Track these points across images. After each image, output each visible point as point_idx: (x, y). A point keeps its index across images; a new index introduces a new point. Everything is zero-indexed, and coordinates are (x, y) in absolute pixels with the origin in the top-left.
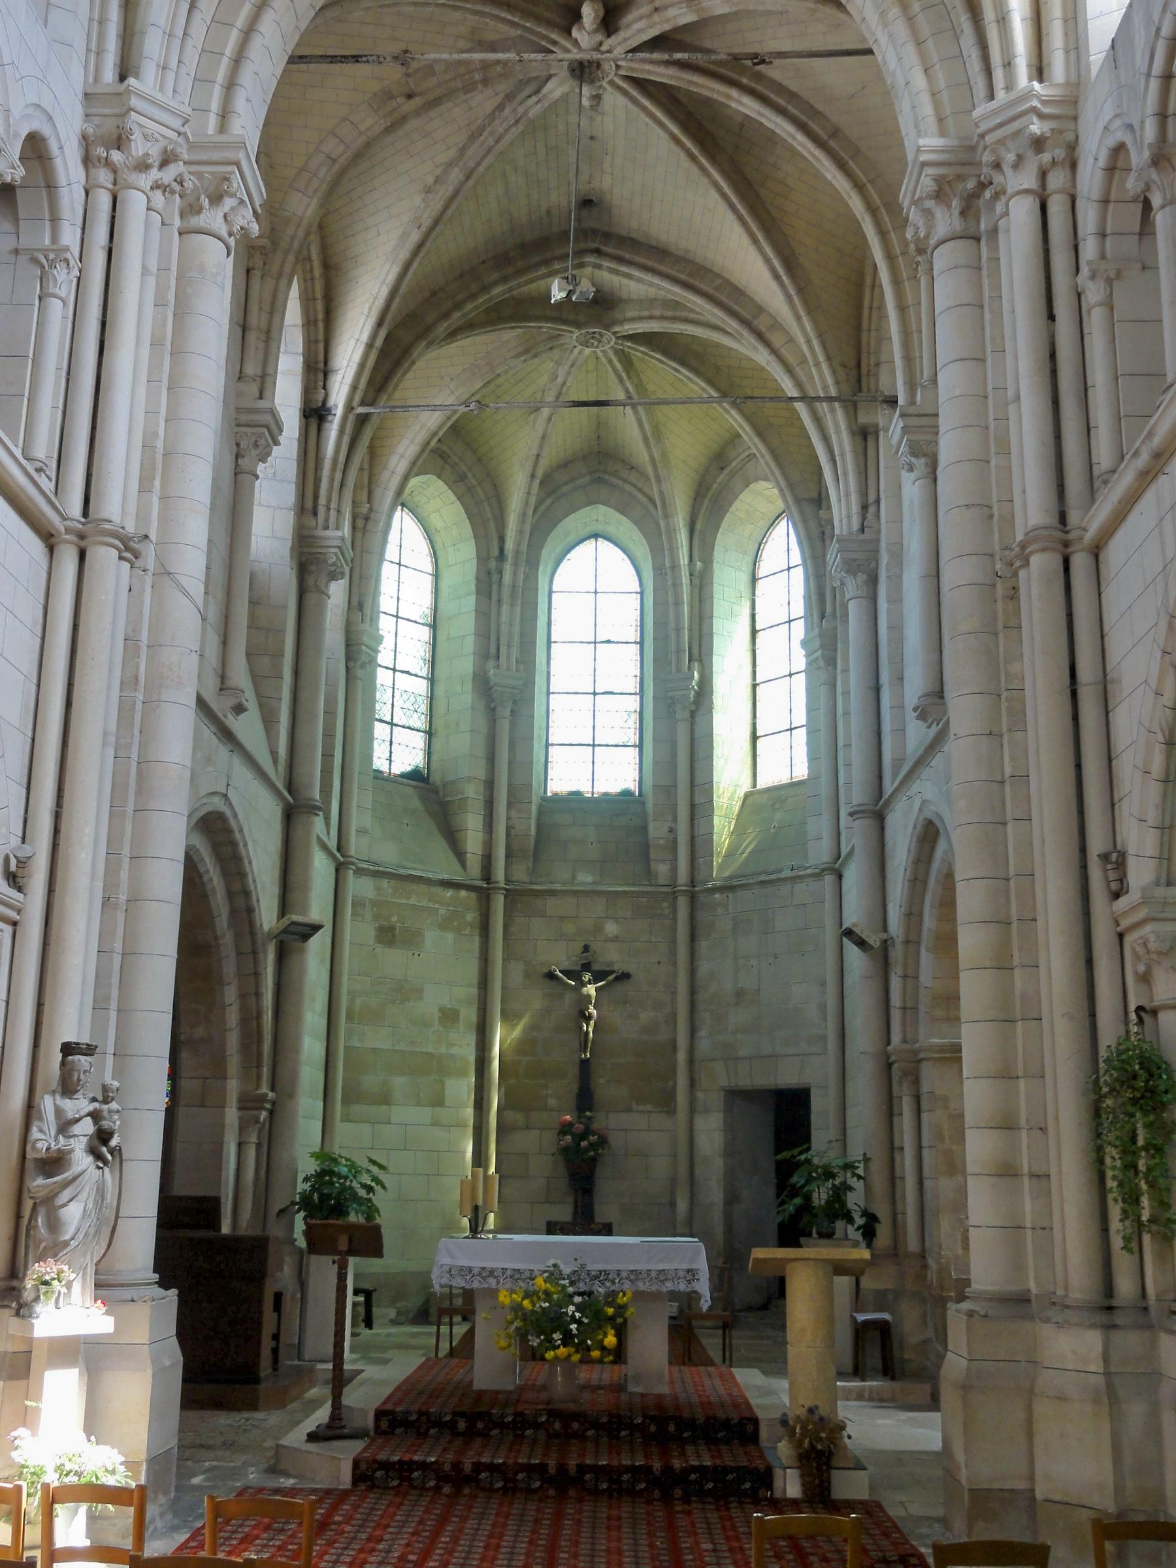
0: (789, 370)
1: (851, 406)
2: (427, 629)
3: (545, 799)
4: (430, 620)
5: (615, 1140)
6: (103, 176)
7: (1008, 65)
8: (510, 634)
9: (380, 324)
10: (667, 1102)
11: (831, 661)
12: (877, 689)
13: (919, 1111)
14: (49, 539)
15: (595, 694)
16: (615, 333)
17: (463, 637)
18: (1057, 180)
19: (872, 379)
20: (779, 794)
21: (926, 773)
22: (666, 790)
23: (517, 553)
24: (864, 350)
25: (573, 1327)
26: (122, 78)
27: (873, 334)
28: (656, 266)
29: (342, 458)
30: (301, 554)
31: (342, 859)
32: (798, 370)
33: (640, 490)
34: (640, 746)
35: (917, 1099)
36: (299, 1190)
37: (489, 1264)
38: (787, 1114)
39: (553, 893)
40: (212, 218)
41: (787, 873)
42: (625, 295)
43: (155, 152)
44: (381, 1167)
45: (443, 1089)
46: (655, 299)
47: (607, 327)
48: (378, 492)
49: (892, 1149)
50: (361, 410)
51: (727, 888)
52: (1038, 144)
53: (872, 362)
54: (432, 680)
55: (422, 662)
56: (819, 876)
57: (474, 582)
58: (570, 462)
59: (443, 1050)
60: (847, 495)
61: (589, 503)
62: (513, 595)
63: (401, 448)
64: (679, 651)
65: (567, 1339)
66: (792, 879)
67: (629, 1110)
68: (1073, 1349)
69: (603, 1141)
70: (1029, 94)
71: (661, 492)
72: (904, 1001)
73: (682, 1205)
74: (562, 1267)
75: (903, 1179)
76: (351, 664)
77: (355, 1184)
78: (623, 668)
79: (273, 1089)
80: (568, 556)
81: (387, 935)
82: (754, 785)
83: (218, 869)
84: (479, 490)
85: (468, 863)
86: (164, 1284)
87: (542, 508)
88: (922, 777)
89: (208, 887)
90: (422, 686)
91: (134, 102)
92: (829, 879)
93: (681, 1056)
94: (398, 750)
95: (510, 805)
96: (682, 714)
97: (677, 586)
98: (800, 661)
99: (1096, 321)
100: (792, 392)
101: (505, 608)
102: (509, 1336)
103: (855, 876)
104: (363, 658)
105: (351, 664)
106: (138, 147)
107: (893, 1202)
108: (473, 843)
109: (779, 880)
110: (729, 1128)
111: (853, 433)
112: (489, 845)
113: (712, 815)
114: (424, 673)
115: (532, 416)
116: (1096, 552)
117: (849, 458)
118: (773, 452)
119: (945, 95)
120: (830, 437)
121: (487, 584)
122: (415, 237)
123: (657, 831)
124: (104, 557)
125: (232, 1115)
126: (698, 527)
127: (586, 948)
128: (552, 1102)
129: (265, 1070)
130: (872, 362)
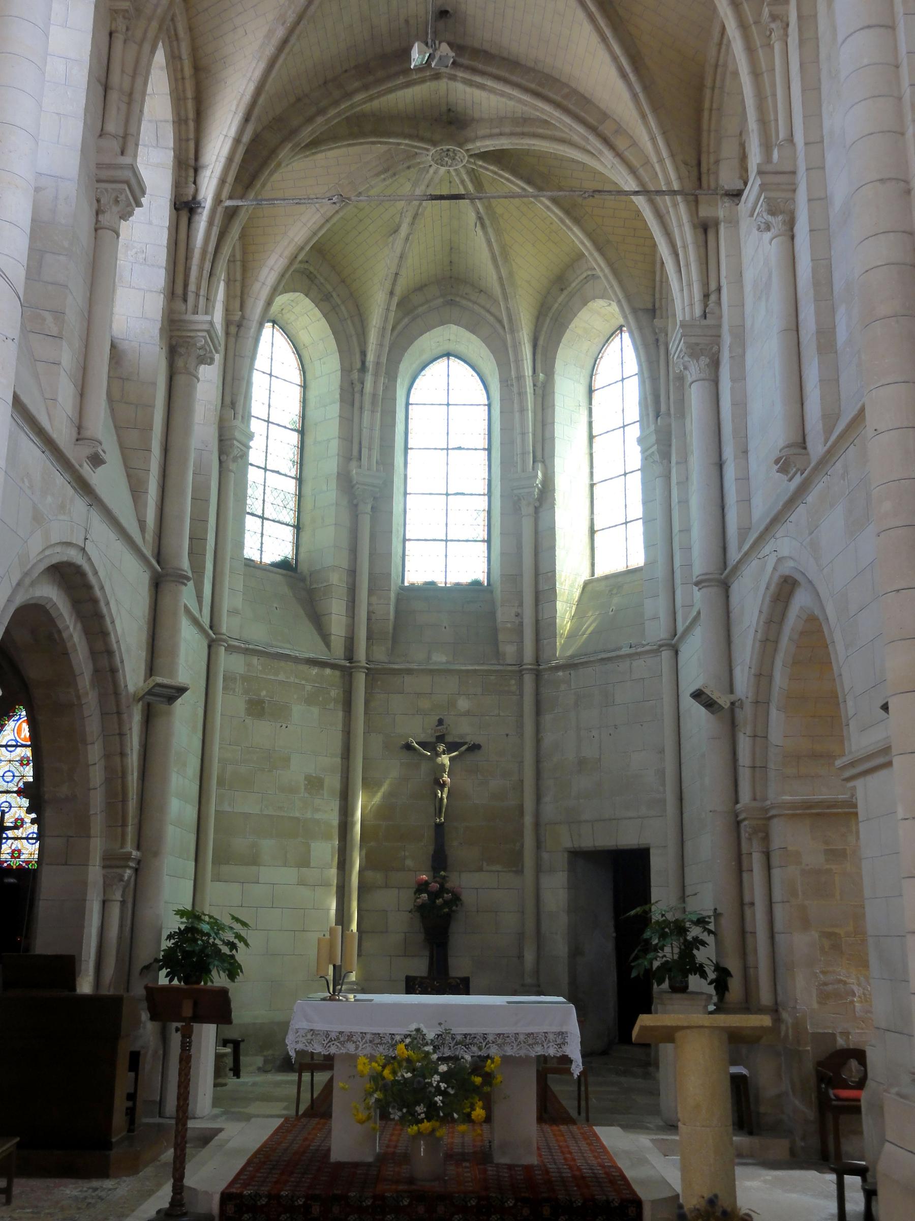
1: (694, 202)
2: (296, 434)
3: (403, 588)
4: (298, 426)
5: (468, 897)
8: (371, 438)
9: (247, 119)
10: (515, 863)
11: (666, 455)
12: (720, 465)
13: (769, 867)
15: (447, 495)
16: (468, 150)
17: (329, 440)
19: (712, 177)
20: (616, 581)
21: (781, 531)
22: (512, 577)
23: (378, 364)
24: (704, 149)
25: (438, 1099)
27: (712, 134)
28: (507, 75)
29: (211, 248)
30: (171, 337)
31: (214, 636)
32: (641, 171)
33: (488, 311)
34: (489, 541)
35: (767, 855)
36: (163, 947)
37: (347, 1028)
38: (626, 872)
39: (409, 672)
41: (626, 651)
42: (477, 115)
44: (244, 924)
45: (309, 851)
46: (506, 117)
47: (460, 145)
48: (249, 303)
49: (742, 905)
50: (229, 203)
51: (571, 665)
53: (712, 160)
55: (291, 464)
56: (657, 651)
57: (338, 391)
58: (426, 285)
59: (309, 815)
60: (690, 285)
62: (374, 403)
63: (271, 262)
64: (524, 453)
66: (629, 656)
67: (480, 869)
69: (457, 898)
71: (508, 308)
72: (754, 759)
73: (529, 957)
74: (425, 1031)
75: (754, 933)
76: (224, 458)
77: (217, 942)
78: (473, 472)
79: (138, 848)
80: (423, 373)
81: (257, 708)
82: (593, 574)
83: (79, 626)
84: (343, 308)
85: (332, 645)
87: (400, 327)
88: (777, 535)
89: (69, 645)
90: (291, 486)
92: (666, 654)
93: (528, 820)
94: (268, 539)
95: (371, 592)
96: (527, 510)
97: (521, 394)
101: (366, 414)
102: (369, 1108)
104: (235, 452)
105: (224, 458)
107: (744, 955)
108: (337, 626)
109: (618, 657)
113: (554, 601)
114: (293, 473)
115: (391, 238)
117: (691, 248)
118: (610, 265)
121: (351, 393)
122: (280, 33)
123: (504, 616)
125: (95, 872)
126: (541, 342)
127: (440, 722)
128: (409, 863)
129: (130, 830)
130: (712, 160)
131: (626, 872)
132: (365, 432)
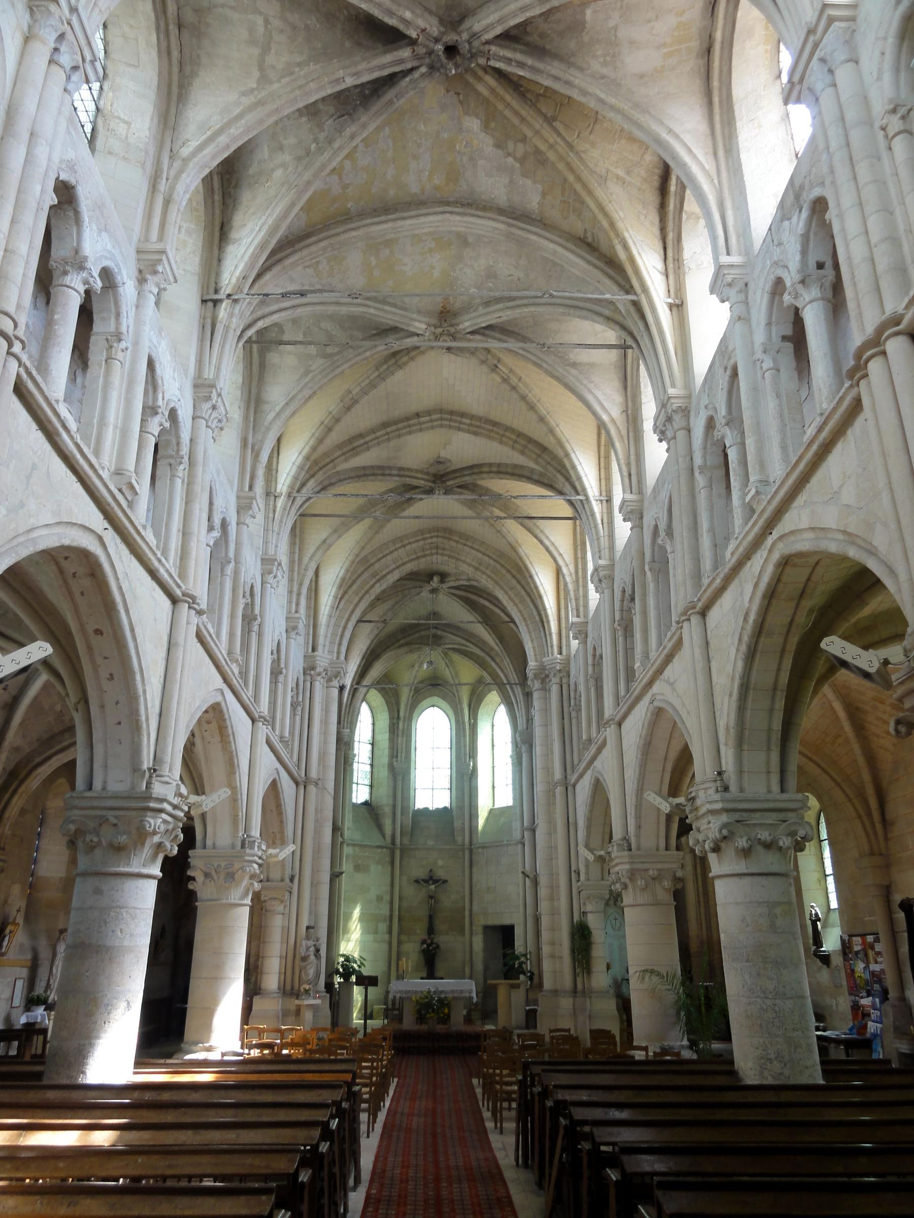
5: (441, 946)
6: (308, 678)
7: (552, 647)
9: (363, 658)
10: (462, 931)
14: (297, 783)
18: (564, 680)
20: (504, 810)
22: (461, 808)
23: (405, 717)
26: (314, 650)
38: (506, 934)
41: (505, 842)
43: (322, 670)
52: (560, 671)
54: (372, 765)
56: (516, 844)
62: (403, 733)
64: (465, 754)
65: (433, 1011)
68: (566, 1003)
69: (438, 947)
70: (556, 658)
73: (467, 971)
81: (357, 868)
86: (327, 992)
90: (368, 768)
92: (520, 846)
93: (467, 913)
94: (360, 794)
95: (402, 814)
96: (466, 778)
97: (464, 729)
98: (510, 761)
106: (318, 670)
108: (388, 831)
110: (485, 941)
111: (523, 695)
116: (574, 786)
119: (537, 649)
123: (457, 824)
124: (312, 789)
127: (431, 871)
128: (418, 931)
131: (506, 934)
132: (399, 746)
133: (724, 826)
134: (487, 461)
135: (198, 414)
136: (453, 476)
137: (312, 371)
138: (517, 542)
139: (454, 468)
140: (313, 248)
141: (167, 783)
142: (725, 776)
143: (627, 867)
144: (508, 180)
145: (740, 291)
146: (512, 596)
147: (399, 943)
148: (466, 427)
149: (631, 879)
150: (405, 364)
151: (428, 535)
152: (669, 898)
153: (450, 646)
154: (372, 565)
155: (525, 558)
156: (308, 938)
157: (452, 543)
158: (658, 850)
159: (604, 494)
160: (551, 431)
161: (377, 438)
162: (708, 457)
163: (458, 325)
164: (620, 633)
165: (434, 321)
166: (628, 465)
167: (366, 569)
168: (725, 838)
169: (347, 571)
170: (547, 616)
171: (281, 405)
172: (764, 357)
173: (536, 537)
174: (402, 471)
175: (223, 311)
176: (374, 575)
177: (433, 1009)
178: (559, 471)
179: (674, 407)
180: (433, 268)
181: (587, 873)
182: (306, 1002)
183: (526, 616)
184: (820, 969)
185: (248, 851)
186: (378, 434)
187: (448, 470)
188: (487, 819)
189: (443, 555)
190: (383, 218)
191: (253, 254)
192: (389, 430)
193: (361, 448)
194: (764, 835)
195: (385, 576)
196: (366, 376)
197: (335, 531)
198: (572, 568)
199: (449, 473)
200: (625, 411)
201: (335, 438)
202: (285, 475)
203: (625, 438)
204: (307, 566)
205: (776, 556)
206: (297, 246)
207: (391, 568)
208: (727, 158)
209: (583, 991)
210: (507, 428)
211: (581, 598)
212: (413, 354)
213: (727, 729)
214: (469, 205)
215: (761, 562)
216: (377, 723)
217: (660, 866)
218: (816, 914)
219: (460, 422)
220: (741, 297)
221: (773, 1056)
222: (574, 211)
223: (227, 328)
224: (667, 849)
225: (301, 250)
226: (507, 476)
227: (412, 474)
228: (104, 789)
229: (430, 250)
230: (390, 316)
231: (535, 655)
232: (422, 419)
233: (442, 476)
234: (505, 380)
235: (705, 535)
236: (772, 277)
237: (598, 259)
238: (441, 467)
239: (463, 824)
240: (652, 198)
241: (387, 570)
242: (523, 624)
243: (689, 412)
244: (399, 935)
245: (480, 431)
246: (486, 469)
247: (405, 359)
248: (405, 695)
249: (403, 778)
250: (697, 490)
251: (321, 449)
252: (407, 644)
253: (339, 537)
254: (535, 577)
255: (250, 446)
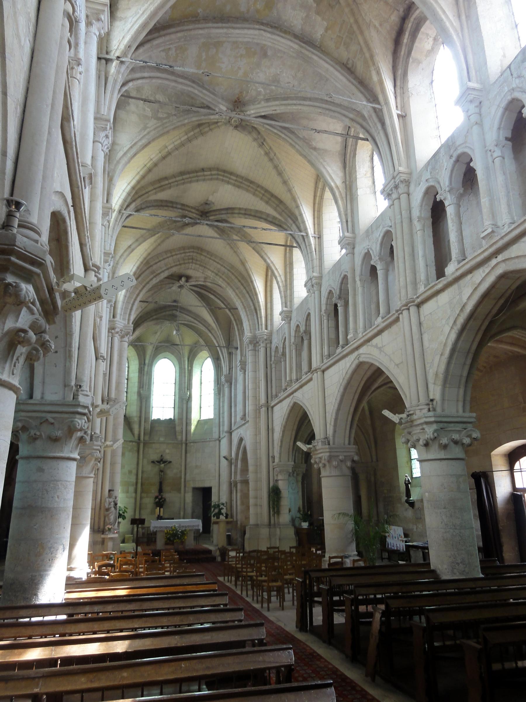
0: (215, 338)
5: (167, 500)
6: (110, 334)
7: (262, 325)
10: (179, 490)
11: (219, 394)
18: (268, 345)
22: (181, 419)
23: (149, 364)
26: (114, 317)
32: (217, 339)
40: (126, 339)
41: (208, 440)
52: (266, 340)
56: (215, 441)
61: (165, 351)
62: (147, 373)
64: (185, 388)
65: (178, 538)
68: (264, 532)
69: (165, 499)
70: (265, 332)
73: (182, 513)
91: (117, 322)
92: (217, 442)
93: (183, 480)
95: (145, 422)
96: (185, 402)
97: (185, 373)
99: (273, 370)
100: (217, 345)
103: (224, 442)
106: (117, 330)
108: (136, 432)
110: (194, 496)
111: (228, 354)
112: (140, 432)
116: (272, 407)
120: (224, 354)
123: (178, 429)
127: (162, 456)
128: (153, 491)
132: (145, 381)
133: (435, 431)
134: (238, 206)
135: (97, 139)
136: (214, 213)
137: (148, 128)
138: (246, 260)
139: (214, 208)
140: (173, 36)
141: (87, 396)
142: (434, 403)
143: (328, 454)
144: (305, 14)
145: (477, 107)
146: (238, 292)
147: (141, 498)
148: (233, 182)
149: (329, 461)
150: (206, 132)
151: (178, 252)
152: (348, 472)
153: (183, 322)
154: (151, 266)
155: (249, 270)
156: (110, 496)
157: (203, 257)
158: (344, 444)
159: (317, 233)
160: (290, 191)
161: (176, 181)
162: (422, 212)
163: (246, 111)
164: (325, 318)
165: (231, 107)
166: (346, 215)
167: (148, 268)
168: (435, 437)
169: (138, 268)
170: (259, 306)
171: (129, 146)
172: (496, 149)
173: (262, 257)
174: (184, 207)
175: (113, 67)
176: (153, 272)
177: (178, 537)
178: (289, 217)
179: (402, 178)
180: (239, 68)
181: (280, 458)
182: (109, 536)
183: (245, 305)
184: (406, 510)
185: (95, 443)
186: (178, 179)
187: (211, 209)
188: (197, 426)
189: (196, 264)
190: (220, 25)
191: (137, 30)
192: (184, 177)
193: (166, 186)
194: (456, 437)
195: (159, 274)
196: (178, 137)
197: (137, 240)
198: (283, 279)
199: (211, 211)
200: (345, 182)
201: (151, 177)
202: (117, 198)
203: (345, 199)
204: (118, 261)
205: (499, 271)
206: (162, 33)
207: (163, 269)
208: (467, 21)
209: (275, 524)
210: (259, 186)
211: (289, 296)
212: (213, 127)
213: (436, 375)
214: (276, 28)
215: (483, 275)
216: (130, 367)
217: (345, 454)
218: (408, 480)
219: (230, 178)
220: (477, 110)
221: (459, 561)
222: (344, 44)
223: (115, 81)
224: (349, 444)
225: (164, 35)
226: (251, 217)
227: (189, 209)
228: (42, 398)
229: (241, 56)
230: (205, 96)
231: (250, 329)
232: (206, 173)
233: (207, 213)
234: (267, 154)
235: (420, 259)
236: (509, 98)
237: (354, 79)
238: (207, 207)
239: (182, 429)
240: (390, 45)
241: (161, 270)
242: (244, 310)
243: (409, 183)
244: (141, 493)
245: (242, 185)
246: (236, 211)
247: (207, 129)
248: (150, 350)
249: (146, 401)
250: (414, 231)
251: (143, 183)
252: (157, 319)
253: (139, 245)
254: (254, 282)
255: (107, 173)
